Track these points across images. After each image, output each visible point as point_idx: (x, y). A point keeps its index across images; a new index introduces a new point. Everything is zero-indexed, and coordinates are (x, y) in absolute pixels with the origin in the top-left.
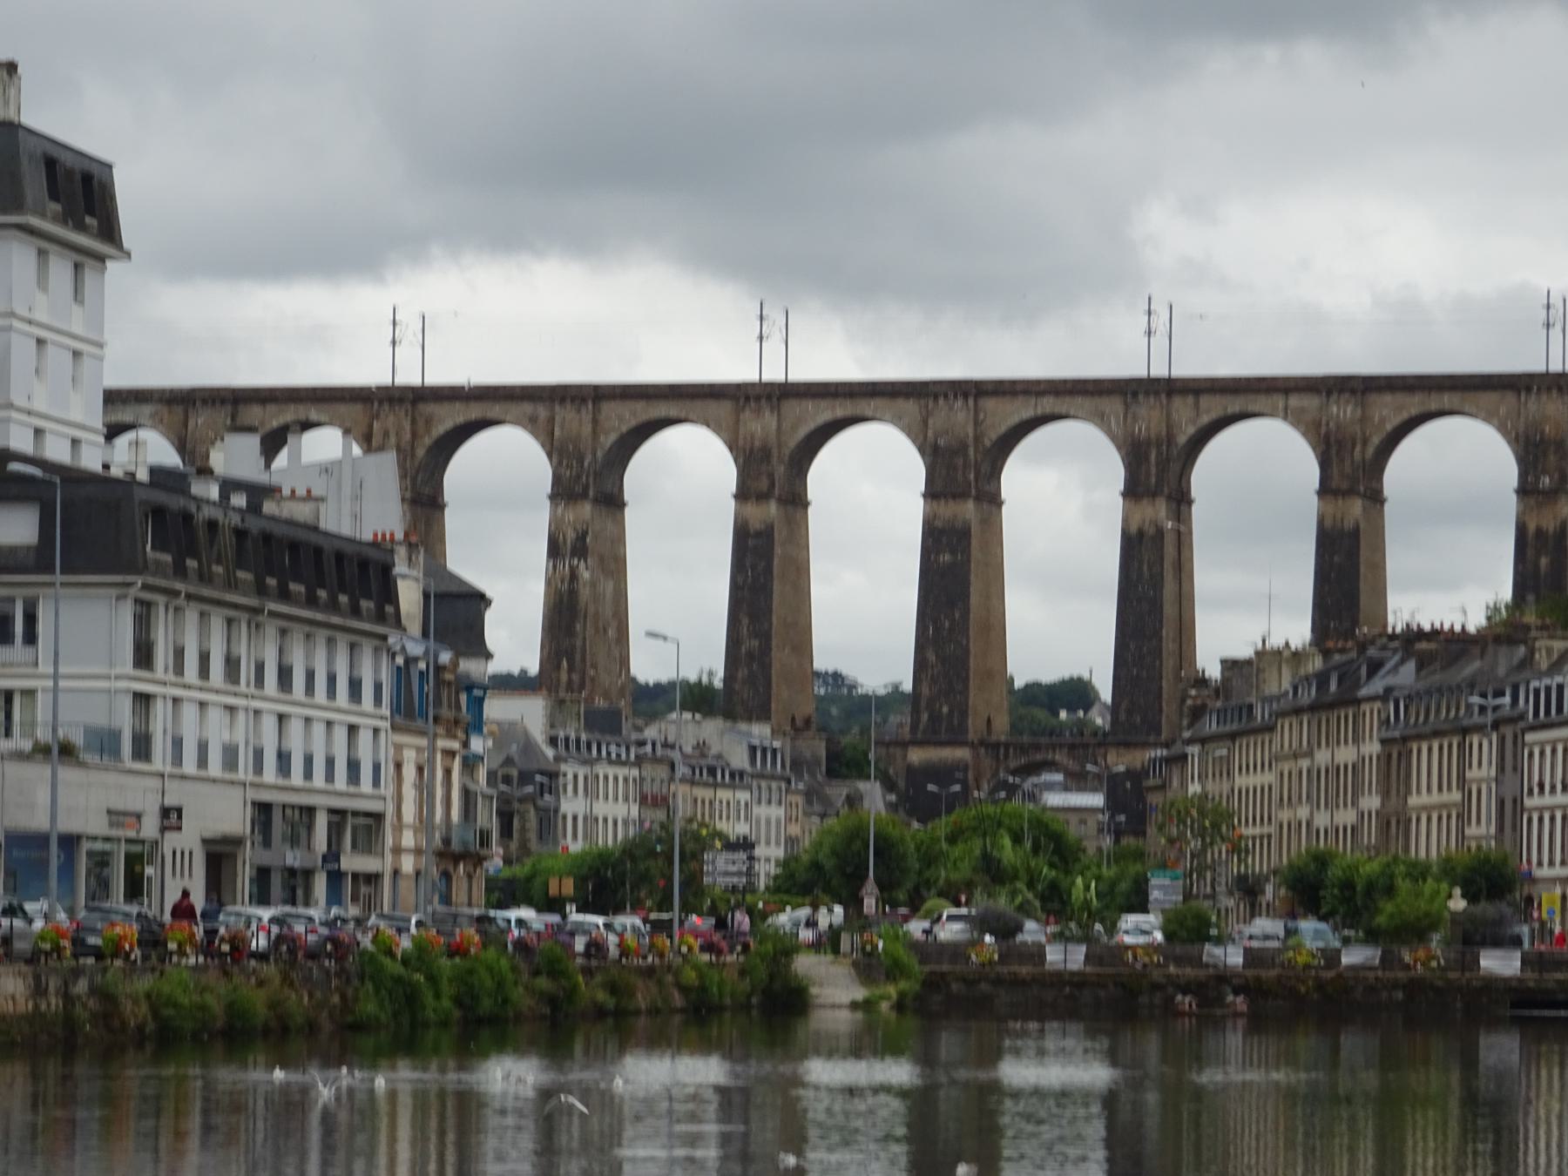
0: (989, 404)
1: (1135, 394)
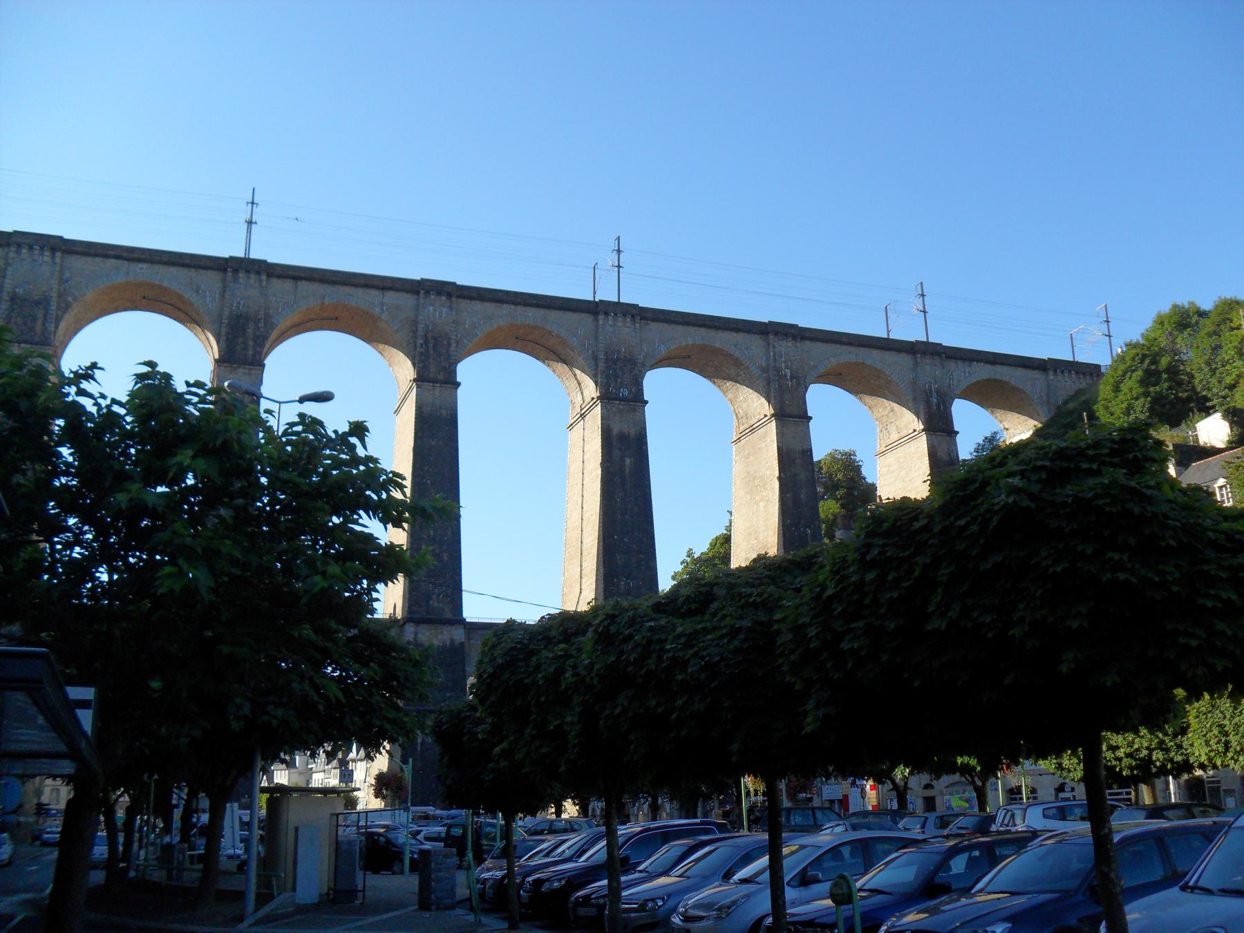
0: (78, 263)
1: (236, 271)
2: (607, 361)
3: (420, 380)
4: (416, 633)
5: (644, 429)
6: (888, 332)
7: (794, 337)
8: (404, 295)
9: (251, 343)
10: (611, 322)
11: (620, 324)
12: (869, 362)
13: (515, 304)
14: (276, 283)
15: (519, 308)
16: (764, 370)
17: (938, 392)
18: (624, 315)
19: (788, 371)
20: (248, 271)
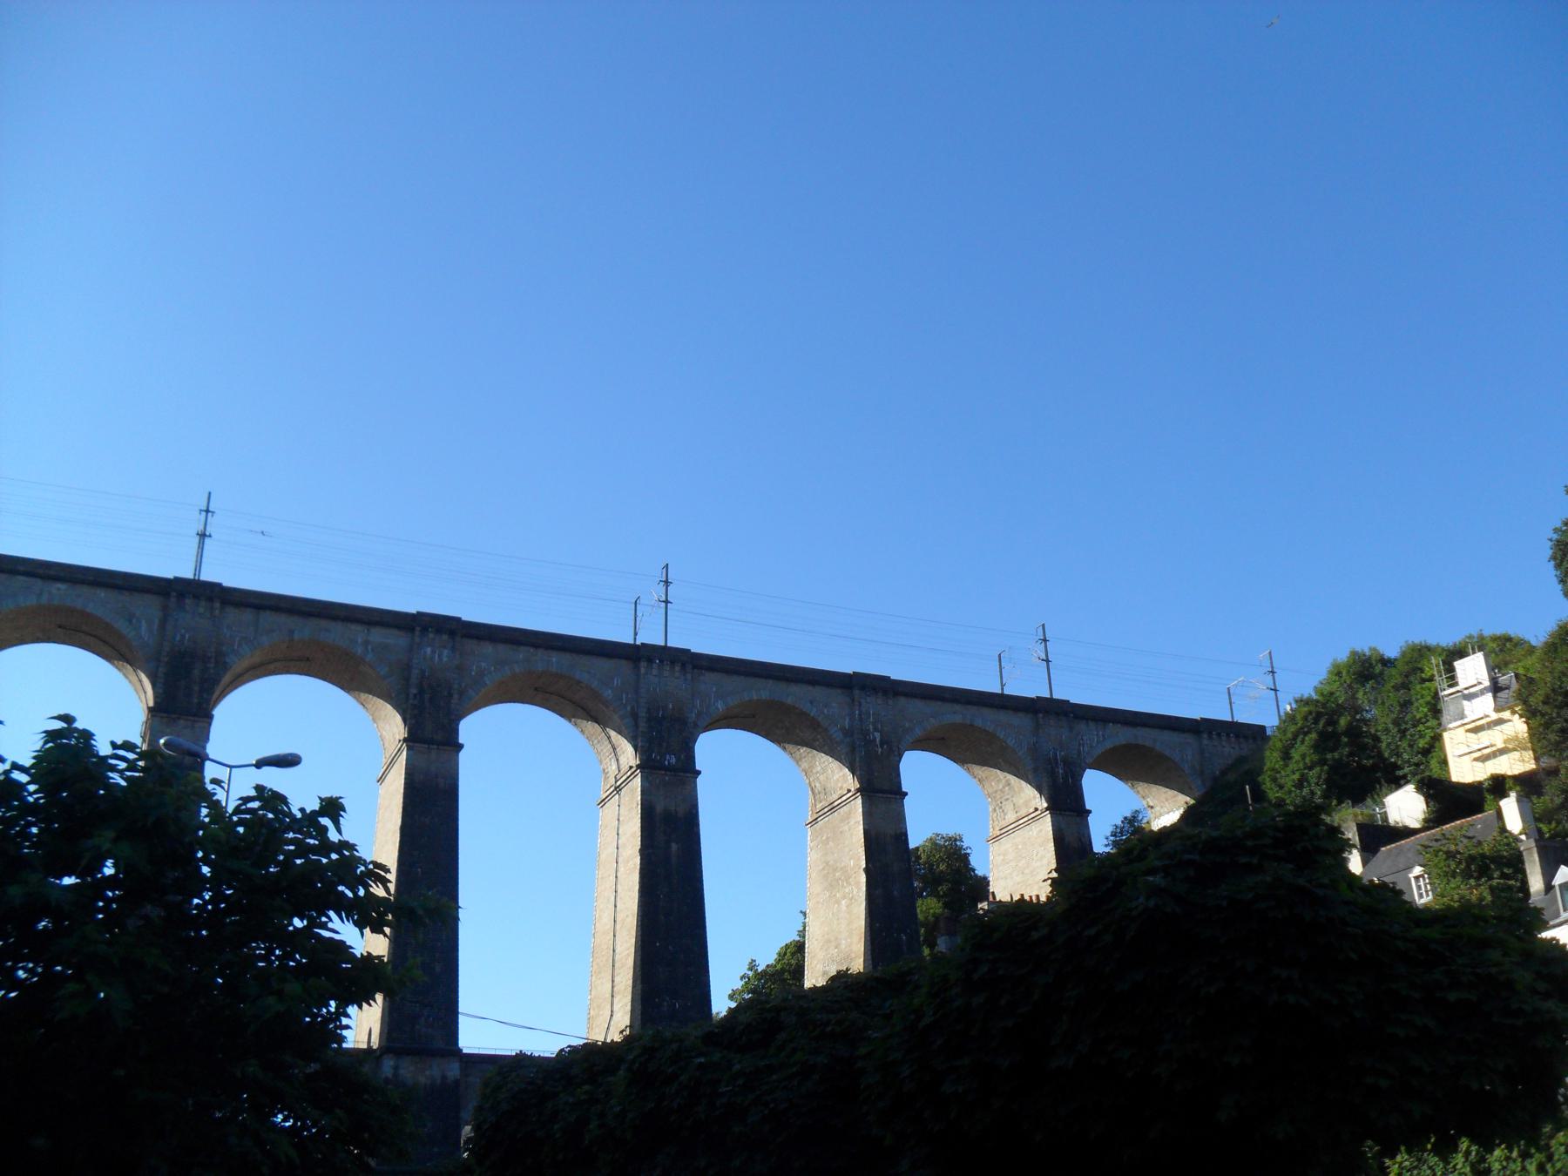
1: (181, 596)
2: (649, 720)
3: (411, 740)
4: (396, 1068)
5: (695, 806)
6: (1003, 686)
7: (885, 692)
8: (396, 632)
9: (196, 688)
10: (655, 672)
11: (666, 673)
12: (978, 723)
13: (536, 646)
14: (233, 615)
15: (540, 652)
16: (848, 733)
17: (1066, 762)
18: (673, 663)
19: (877, 735)
20: (196, 597)
